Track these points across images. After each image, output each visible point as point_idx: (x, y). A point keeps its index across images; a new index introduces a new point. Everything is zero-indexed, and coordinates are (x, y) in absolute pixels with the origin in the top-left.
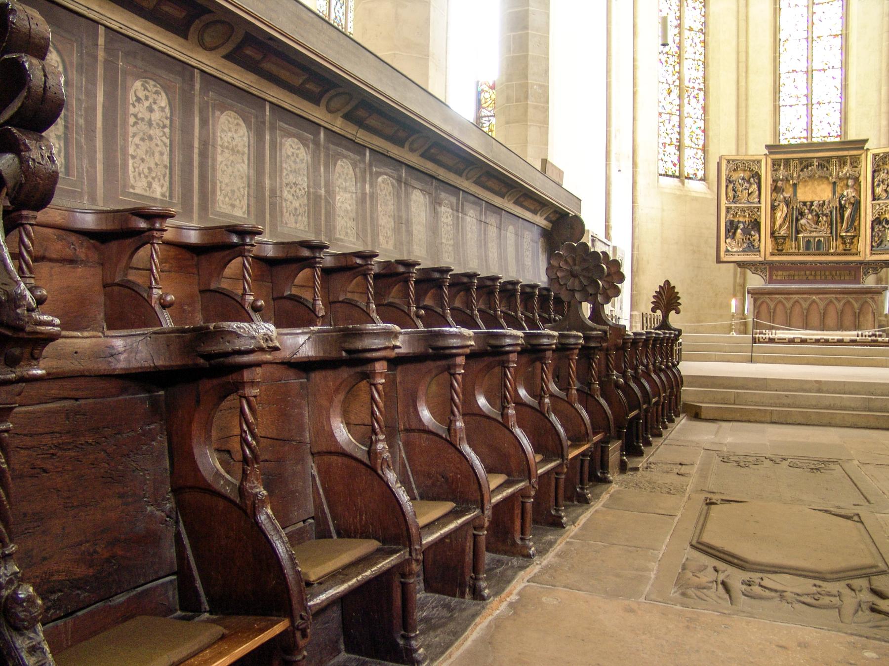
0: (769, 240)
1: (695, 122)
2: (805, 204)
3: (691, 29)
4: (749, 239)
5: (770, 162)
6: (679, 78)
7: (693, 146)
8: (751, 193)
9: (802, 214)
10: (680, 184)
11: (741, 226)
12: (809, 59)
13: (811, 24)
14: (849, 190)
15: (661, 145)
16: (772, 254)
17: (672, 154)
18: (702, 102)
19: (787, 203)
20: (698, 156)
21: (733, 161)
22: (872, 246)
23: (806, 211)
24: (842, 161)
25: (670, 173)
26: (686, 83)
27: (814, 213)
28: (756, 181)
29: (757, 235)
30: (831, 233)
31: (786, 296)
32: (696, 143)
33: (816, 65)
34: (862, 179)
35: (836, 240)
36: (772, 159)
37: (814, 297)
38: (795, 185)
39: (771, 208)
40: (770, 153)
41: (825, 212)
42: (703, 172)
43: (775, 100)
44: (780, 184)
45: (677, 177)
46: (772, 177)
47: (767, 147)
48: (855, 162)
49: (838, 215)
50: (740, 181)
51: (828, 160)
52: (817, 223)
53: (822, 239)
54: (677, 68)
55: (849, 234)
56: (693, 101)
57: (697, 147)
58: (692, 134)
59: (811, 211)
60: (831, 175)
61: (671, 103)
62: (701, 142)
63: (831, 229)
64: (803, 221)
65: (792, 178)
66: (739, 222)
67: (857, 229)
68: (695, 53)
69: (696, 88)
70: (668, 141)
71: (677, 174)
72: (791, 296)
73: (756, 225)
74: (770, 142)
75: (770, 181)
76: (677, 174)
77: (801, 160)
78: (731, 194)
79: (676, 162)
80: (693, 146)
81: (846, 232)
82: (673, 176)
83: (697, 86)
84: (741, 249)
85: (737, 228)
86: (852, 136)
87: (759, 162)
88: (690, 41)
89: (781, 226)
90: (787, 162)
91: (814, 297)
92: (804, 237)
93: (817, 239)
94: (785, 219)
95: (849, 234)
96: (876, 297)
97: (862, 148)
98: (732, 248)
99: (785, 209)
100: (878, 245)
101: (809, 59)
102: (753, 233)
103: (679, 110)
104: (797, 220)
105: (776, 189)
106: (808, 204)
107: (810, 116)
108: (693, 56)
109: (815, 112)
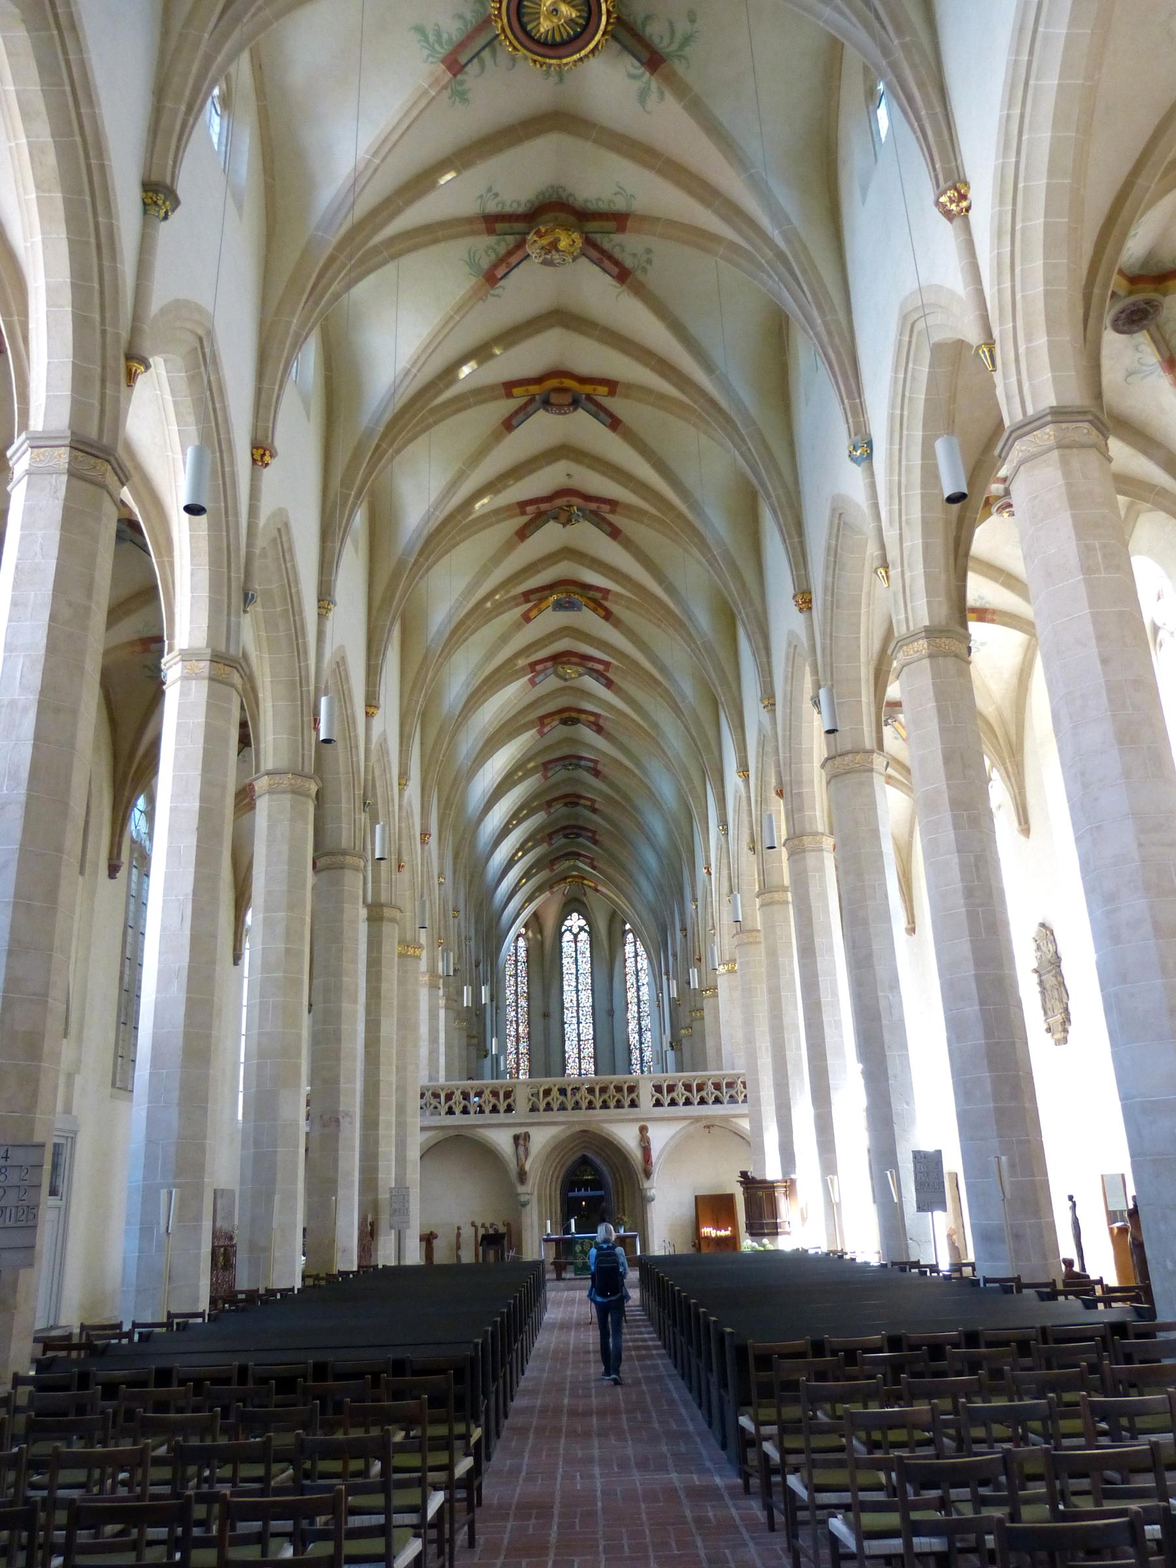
12: (580, 1068)
33: (583, 1072)
101: (580, 1068)
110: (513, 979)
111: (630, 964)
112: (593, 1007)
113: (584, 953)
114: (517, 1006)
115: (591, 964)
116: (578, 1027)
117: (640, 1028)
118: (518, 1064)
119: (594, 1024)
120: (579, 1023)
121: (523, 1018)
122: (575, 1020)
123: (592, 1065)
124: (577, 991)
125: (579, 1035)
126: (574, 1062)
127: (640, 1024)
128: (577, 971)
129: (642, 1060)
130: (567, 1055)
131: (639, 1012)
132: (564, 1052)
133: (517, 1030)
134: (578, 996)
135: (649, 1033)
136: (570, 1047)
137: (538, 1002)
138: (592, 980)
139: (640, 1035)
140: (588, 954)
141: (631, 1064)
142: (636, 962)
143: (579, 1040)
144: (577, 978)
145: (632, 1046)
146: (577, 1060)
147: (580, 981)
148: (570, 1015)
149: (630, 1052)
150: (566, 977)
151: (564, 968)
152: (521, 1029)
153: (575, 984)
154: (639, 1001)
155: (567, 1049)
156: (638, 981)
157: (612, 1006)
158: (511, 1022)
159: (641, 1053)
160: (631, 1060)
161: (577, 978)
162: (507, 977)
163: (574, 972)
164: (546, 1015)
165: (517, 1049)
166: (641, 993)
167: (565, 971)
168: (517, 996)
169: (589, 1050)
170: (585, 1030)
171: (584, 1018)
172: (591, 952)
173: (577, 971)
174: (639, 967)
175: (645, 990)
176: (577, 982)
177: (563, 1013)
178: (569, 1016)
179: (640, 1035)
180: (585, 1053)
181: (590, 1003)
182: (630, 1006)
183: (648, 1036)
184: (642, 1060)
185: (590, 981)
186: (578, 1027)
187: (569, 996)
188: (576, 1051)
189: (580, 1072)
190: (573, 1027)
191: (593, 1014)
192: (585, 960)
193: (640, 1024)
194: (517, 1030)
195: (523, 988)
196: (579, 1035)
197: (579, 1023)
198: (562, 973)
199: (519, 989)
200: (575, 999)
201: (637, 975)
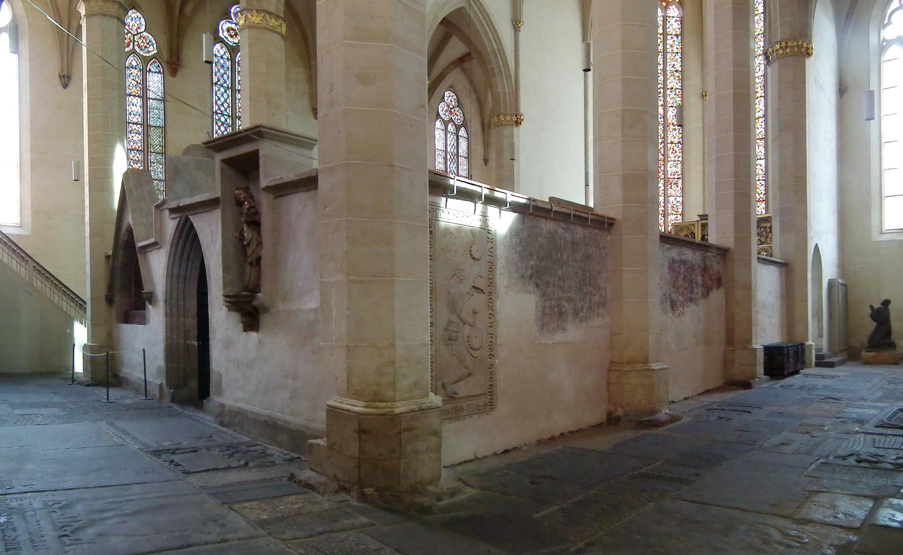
3: (672, 143)
7: (675, 213)
36: (701, 223)
40: (701, 220)
46: (701, 233)
47: (699, 216)
62: (680, 210)
69: (676, 178)
74: (701, 213)
80: (675, 213)
86: (706, 214)
87: (694, 225)
88: (671, 150)
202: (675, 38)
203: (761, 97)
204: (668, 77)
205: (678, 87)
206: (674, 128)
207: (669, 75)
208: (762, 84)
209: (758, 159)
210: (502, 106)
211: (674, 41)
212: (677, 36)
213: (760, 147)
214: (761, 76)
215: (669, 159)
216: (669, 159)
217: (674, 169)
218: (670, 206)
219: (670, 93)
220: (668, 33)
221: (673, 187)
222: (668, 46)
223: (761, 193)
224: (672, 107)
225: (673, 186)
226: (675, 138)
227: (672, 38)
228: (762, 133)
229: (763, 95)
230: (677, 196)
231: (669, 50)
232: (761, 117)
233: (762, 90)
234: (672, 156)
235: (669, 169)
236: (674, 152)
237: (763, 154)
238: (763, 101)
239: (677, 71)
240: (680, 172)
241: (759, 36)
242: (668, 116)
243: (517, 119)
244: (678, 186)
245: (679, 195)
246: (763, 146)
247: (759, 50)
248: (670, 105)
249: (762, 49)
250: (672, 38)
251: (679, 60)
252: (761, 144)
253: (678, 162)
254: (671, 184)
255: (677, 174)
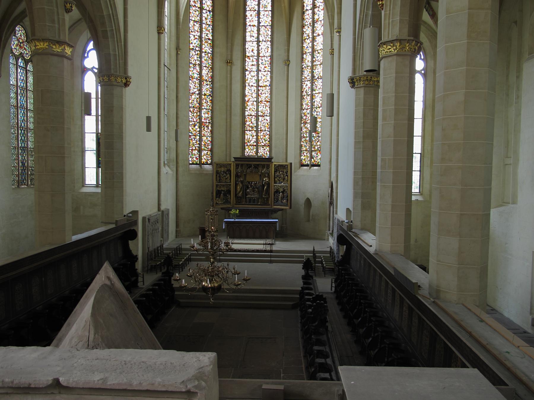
0: (235, 198)
1: (207, 138)
2: (249, 182)
3: (205, 95)
4: (226, 198)
5: (235, 164)
6: (199, 119)
7: (206, 149)
8: (227, 178)
9: (248, 188)
10: (199, 167)
11: (223, 192)
12: (257, 111)
13: (258, 96)
14: (266, 178)
15: (190, 150)
16: (236, 204)
17: (196, 154)
18: (210, 128)
19: (242, 182)
20: (209, 154)
21: (219, 164)
22: (274, 202)
23: (249, 186)
24: (263, 166)
25: (195, 163)
26: (203, 120)
27: (253, 187)
28: (229, 173)
29: (229, 196)
30: (259, 196)
31: (239, 224)
32: (208, 147)
33: (260, 114)
34: (270, 174)
35: (261, 199)
37: (251, 225)
38: (245, 175)
39: (235, 184)
41: (257, 187)
42: (210, 161)
43: (243, 128)
44: (239, 174)
45: (198, 164)
46: (236, 171)
48: (268, 167)
49: (262, 190)
50: (222, 173)
51: (258, 165)
52: (254, 191)
53: (255, 198)
54: (198, 114)
55: (265, 197)
56: (206, 128)
57: (208, 149)
58: (206, 144)
59: (251, 186)
60: (259, 171)
61: (195, 131)
63: (259, 194)
64: (248, 190)
65: (244, 172)
66: (222, 190)
67: (269, 195)
68: (207, 106)
69: (208, 122)
70: (194, 148)
71: (198, 163)
72: (242, 224)
73: (229, 192)
75: (235, 172)
76: (198, 163)
77: (247, 165)
78: (218, 179)
79: (198, 157)
80: (206, 149)
81: (265, 196)
82: (197, 164)
83: (208, 121)
84: (223, 202)
85: (221, 193)
87: (230, 164)
88: (205, 101)
89: (239, 192)
90: (242, 165)
91: (251, 225)
92: (248, 197)
93: (253, 198)
94: (241, 189)
95: (265, 197)
96: (274, 225)
97: (271, 161)
98: (219, 202)
99: (241, 185)
100: (277, 202)
101: (257, 111)
102: (228, 195)
103: (199, 133)
104: (246, 190)
105: (237, 176)
106: (251, 183)
107: (257, 136)
108: (206, 107)
109: (259, 134)
110: (197, 26)
111: (308, 15)
112: (272, 57)
113: (266, 7)
114: (201, 51)
115: (272, 17)
116: (258, 75)
117: (313, 76)
118: (200, 104)
119: (271, 72)
120: (258, 71)
121: (206, 61)
122: (255, 68)
123: (267, 108)
124: (258, 42)
125: (258, 81)
126: (252, 104)
127: (312, 72)
128: (259, 23)
129: (312, 105)
130: (247, 99)
131: (313, 62)
132: (244, 95)
133: (200, 74)
134: (259, 46)
135: (321, 81)
136: (250, 92)
137: (221, 50)
138: (272, 32)
139: (312, 83)
140: (269, 8)
141: (302, 109)
142: (314, 13)
143: (258, 86)
144: (259, 30)
145: (304, 93)
146: (255, 103)
147: (261, 33)
148: (251, 63)
149: (302, 98)
150: (249, 29)
151: (248, 20)
152: (204, 72)
153: (256, 35)
154: (313, 50)
155: (247, 93)
156: (313, 32)
157: (288, 56)
158: (195, 65)
159: (312, 99)
160: (302, 105)
161: (259, 30)
162: (192, 22)
163: (256, 23)
164: (229, 62)
165: (200, 90)
166: (315, 44)
167: (248, 24)
168: (201, 41)
169: (265, 95)
170: (263, 78)
171: (263, 67)
172: (272, 6)
173: (259, 23)
174: (316, 17)
175: (320, 40)
176: (259, 34)
177: (244, 61)
178: (250, 64)
179: (312, 83)
180: (262, 98)
181: (269, 54)
182: (305, 56)
183: (319, 84)
184: (312, 105)
185: (270, 33)
186: (258, 75)
187: (251, 47)
188: (254, 95)
189: (257, 114)
190: (252, 74)
191: (271, 63)
192: (267, 13)
193: (312, 72)
194: (200, 74)
195: (208, 34)
196: (258, 81)
197: (258, 71)
198: (245, 24)
199: (203, 35)
200: (255, 49)
201: (313, 27)
202: (208, 13)
203: (268, 71)
204: (203, 43)
205: (210, 52)
206: (207, 83)
207: (204, 41)
208: (269, 62)
209: (265, 116)
210: (112, 67)
211: (208, 15)
212: (209, 11)
213: (267, 107)
214: (269, 56)
215: (203, 107)
216: (203, 107)
217: (207, 115)
218: (203, 143)
219: (204, 56)
220: (204, 8)
221: (205, 129)
222: (204, 19)
223: (267, 140)
224: (206, 66)
225: (206, 128)
226: (207, 91)
227: (206, 12)
228: (268, 97)
229: (270, 70)
230: (208, 136)
231: (204, 22)
232: (267, 86)
233: (269, 66)
234: (205, 105)
235: (203, 115)
236: (206, 102)
237: (268, 113)
238: (269, 75)
239: (209, 39)
240: (210, 118)
241: (268, 27)
242: (203, 73)
243: (127, 81)
244: (208, 128)
245: (209, 136)
246: (269, 107)
247: (267, 37)
248: (204, 65)
249: (270, 37)
250: (206, 12)
251: (211, 31)
252: (268, 105)
253: (209, 110)
254: (204, 127)
255: (208, 119)
